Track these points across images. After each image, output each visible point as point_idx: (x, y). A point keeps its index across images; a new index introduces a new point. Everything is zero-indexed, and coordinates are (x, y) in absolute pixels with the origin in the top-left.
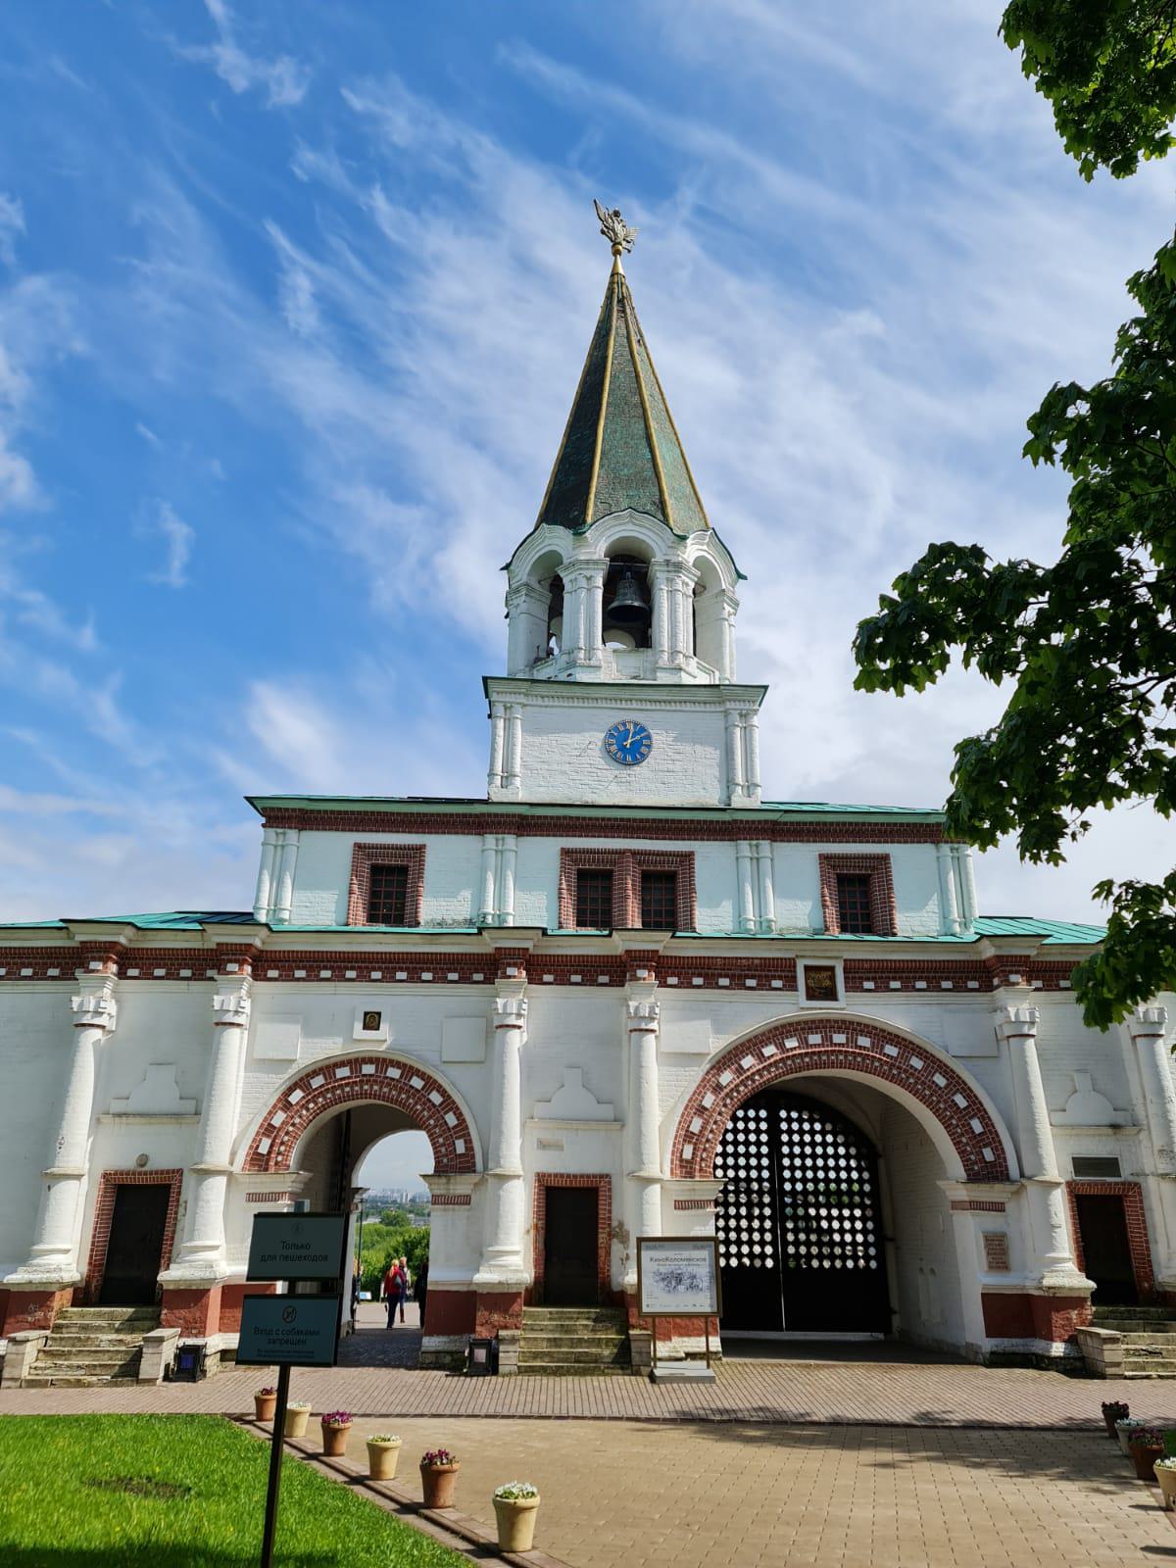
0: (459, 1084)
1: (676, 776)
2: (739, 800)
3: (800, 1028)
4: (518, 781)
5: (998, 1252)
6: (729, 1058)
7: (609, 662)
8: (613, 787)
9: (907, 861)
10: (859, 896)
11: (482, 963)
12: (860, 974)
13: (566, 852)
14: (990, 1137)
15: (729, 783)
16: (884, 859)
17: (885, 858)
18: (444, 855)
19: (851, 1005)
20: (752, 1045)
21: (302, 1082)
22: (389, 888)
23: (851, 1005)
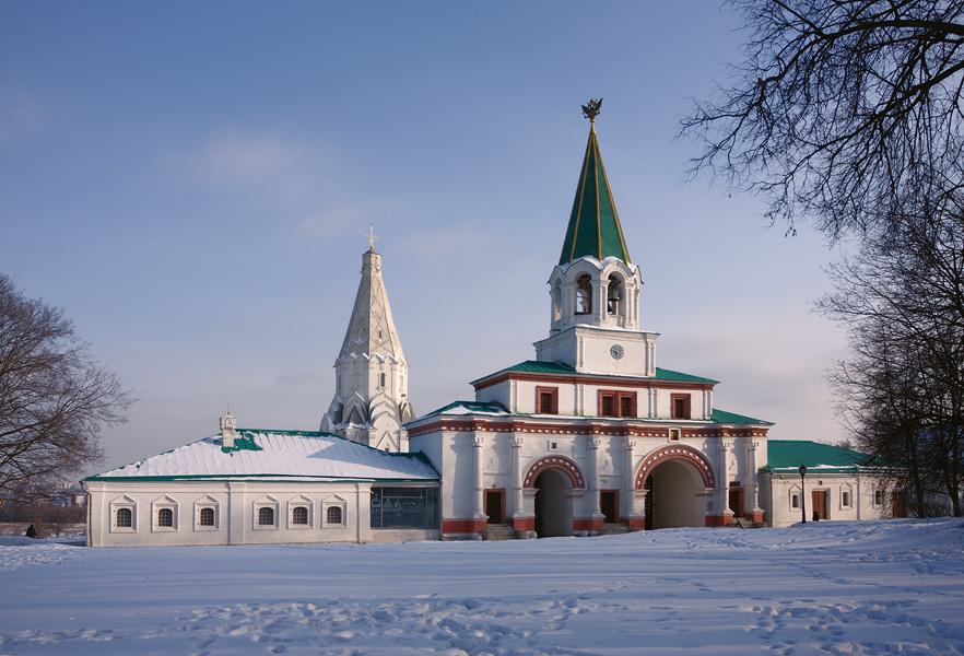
0: (577, 462)
1: (631, 366)
2: (652, 374)
3: (666, 448)
4: (584, 365)
5: (710, 505)
6: (651, 458)
7: (610, 322)
8: (612, 367)
9: (696, 397)
10: (681, 407)
11: (584, 429)
12: (685, 432)
13: (599, 390)
14: (713, 478)
15: (647, 368)
16: (689, 395)
17: (689, 395)
18: (565, 392)
19: (682, 441)
20: (657, 453)
21: (536, 464)
22: (548, 402)
23: (682, 441)
